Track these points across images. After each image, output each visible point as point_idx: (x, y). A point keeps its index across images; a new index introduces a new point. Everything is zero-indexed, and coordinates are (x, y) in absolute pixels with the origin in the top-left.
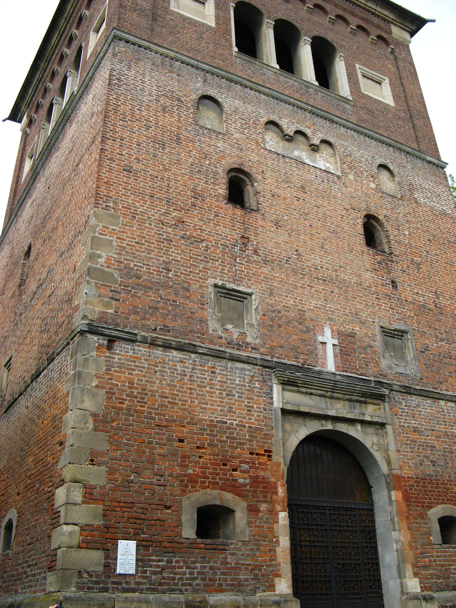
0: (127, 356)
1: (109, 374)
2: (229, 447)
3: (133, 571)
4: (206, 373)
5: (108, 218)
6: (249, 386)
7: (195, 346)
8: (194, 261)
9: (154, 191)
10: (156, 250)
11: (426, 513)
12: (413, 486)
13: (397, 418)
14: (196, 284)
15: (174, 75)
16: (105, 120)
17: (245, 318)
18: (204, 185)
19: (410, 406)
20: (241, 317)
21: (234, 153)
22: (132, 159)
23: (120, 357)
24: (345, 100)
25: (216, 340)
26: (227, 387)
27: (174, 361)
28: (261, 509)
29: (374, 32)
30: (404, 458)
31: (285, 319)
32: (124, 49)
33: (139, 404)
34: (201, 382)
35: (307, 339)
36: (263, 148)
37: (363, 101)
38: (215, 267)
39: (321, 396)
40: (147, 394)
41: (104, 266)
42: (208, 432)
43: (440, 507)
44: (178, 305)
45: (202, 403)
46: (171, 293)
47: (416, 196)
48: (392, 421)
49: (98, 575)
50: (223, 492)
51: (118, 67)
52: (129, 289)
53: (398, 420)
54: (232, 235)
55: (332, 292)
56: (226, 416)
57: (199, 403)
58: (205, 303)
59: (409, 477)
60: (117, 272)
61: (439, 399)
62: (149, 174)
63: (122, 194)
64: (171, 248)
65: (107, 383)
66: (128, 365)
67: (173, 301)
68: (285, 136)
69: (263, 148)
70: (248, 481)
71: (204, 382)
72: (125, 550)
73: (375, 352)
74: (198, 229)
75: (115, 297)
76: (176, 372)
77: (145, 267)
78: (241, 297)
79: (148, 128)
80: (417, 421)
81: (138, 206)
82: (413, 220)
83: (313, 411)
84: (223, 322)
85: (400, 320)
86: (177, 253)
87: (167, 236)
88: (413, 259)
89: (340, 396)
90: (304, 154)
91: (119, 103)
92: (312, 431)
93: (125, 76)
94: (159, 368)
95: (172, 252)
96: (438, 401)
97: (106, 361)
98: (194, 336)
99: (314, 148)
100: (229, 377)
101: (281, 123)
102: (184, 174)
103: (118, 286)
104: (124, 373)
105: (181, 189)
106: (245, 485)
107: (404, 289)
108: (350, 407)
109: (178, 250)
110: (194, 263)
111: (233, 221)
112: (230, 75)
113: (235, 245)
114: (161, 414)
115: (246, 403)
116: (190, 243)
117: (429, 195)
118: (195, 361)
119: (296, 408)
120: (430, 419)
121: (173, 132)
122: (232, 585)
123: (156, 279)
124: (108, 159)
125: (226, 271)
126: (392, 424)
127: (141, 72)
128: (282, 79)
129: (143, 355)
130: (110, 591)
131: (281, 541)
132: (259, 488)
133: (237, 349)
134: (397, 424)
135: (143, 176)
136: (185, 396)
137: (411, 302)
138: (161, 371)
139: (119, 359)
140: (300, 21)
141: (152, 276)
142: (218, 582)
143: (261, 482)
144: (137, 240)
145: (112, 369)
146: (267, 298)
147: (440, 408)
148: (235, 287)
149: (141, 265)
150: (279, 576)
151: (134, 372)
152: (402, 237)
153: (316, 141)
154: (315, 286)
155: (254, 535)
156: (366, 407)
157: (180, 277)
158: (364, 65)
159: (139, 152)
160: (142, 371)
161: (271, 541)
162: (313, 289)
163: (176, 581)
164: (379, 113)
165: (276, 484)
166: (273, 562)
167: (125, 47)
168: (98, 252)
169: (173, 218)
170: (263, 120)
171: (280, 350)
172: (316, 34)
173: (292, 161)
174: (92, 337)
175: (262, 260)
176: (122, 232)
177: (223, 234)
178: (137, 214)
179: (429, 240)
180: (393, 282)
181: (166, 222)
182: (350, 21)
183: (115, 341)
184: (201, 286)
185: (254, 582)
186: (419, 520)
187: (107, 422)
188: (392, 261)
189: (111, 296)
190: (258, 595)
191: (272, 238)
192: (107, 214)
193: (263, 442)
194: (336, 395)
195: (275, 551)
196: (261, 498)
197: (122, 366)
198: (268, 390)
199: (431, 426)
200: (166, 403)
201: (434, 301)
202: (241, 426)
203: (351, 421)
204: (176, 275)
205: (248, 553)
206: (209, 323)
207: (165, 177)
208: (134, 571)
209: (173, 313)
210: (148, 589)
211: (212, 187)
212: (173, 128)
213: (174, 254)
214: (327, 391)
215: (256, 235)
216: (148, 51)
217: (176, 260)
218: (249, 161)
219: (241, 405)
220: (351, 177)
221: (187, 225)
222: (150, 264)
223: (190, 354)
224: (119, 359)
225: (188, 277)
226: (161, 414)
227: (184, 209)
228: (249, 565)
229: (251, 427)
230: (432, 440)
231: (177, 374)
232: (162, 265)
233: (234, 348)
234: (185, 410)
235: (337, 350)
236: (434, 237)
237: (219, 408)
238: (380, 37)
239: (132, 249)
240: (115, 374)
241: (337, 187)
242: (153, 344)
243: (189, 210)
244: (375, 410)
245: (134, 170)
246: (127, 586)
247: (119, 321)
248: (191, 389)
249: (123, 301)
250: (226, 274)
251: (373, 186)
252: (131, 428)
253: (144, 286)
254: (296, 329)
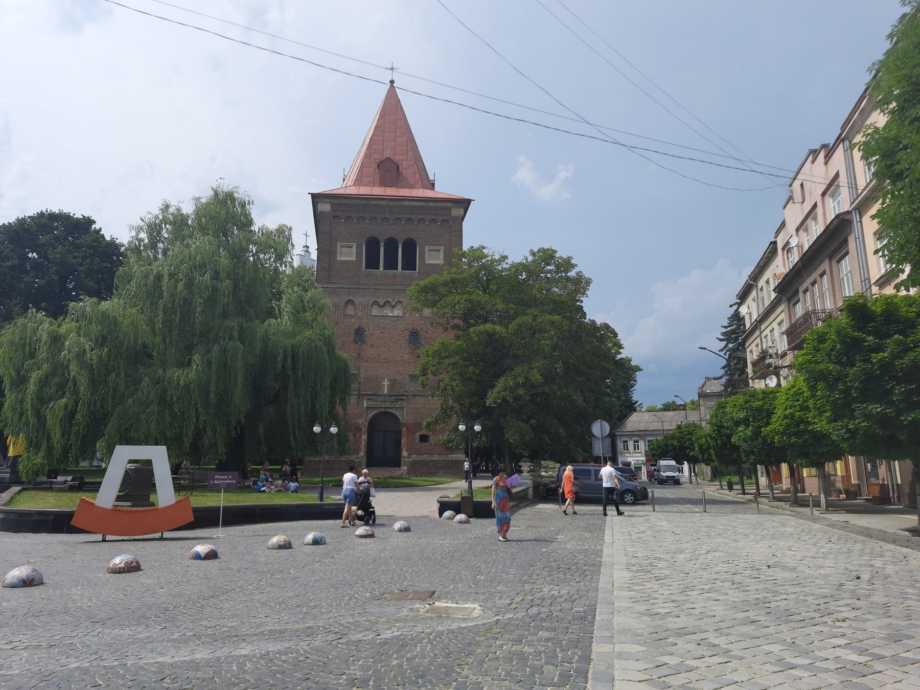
99: (393, 307)
153: (393, 304)
203: (392, 408)
251: (418, 315)
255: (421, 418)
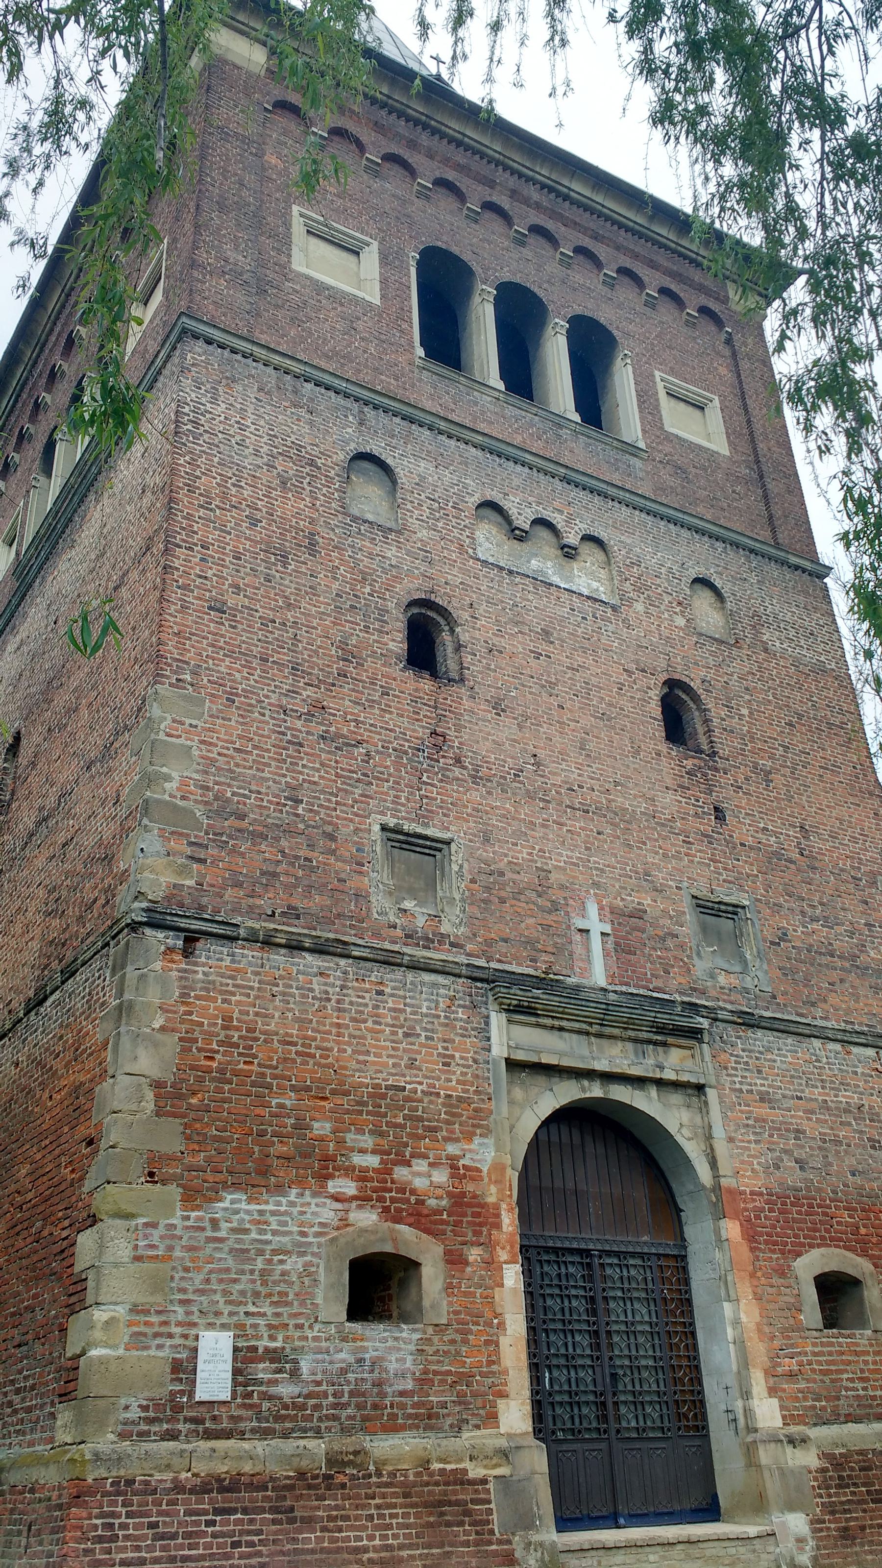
0: (221, 968)
1: (187, 1004)
2: (409, 1135)
3: (226, 1396)
4: (367, 995)
5: (182, 703)
6: (446, 1017)
7: (345, 943)
8: (343, 783)
9: (267, 649)
10: (273, 763)
11: (789, 1266)
12: (762, 1210)
13: (728, 1075)
14: (348, 826)
15: (302, 412)
16: (171, 508)
17: (438, 888)
18: (361, 634)
19: (750, 1051)
20: (431, 886)
21: (417, 568)
22: (226, 587)
23: (206, 969)
24: (631, 449)
25: (385, 932)
26: (405, 1020)
27: (308, 974)
28: (471, 1259)
29: (693, 301)
30: (742, 1154)
31: (511, 888)
32: (203, 358)
33: (242, 1059)
34: (357, 1012)
35: (553, 924)
36: (471, 557)
37: (668, 449)
38: (382, 793)
39: (579, 1032)
40: (256, 1039)
41: (175, 797)
42: (371, 1108)
43: (816, 1253)
44: (314, 867)
45: (360, 1053)
46: (302, 844)
47: (765, 638)
48: (718, 1081)
49: (159, 1404)
50: (398, 1226)
51: (193, 395)
52: (224, 838)
53: (729, 1079)
54: (414, 731)
55: (599, 833)
56: (404, 1076)
57: (354, 1052)
58: (365, 862)
59: (752, 1193)
60: (201, 807)
61: (810, 1036)
62: (258, 615)
63: (207, 656)
64: (302, 759)
65: (182, 1022)
66: (221, 985)
67: (306, 859)
68: (513, 531)
69: (471, 557)
70: (444, 1203)
71: (362, 1012)
72: (211, 1352)
73: (682, 946)
74: (351, 720)
75: (196, 855)
76: (311, 995)
77: (254, 796)
78: (430, 848)
79: (254, 522)
80: (766, 1079)
81: (239, 679)
82: (759, 685)
83: (566, 1062)
84: (396, 893)
85: (730, 882)
86: (313, 768)
87: (293, 735)
88: (758, 764)
89: (616, 1032)
90: (549, 564)
91: (198, 473)
92: (564, 1100)
93: (208, 416)
94: (281, 988)
95: (304, 766)
96: (807, 1040)
97: (181, 978)
98: (344, 926)
99: (569, 553)
100: (408, 1000)
101: (505, 504)
102: (323, 613)
103: (202, 834)
104: (215, 1000)
105: (319, 643)
106: (439, 1212)
107: (740, 822)
108: (636, 1053)
109: (314, 762)
110: (345, 787)
111: (416, 702)
112: (410, 410)
113: (419, 750)
114: (283, 1077)
115: (440, 1050)
116: (336, 748)
117: (792, 633)
118: (345, 973)
119: (534, 1059)
120: (792, 1077)
121: (303, 531)
122: (416, 1416)
123: (274, 818)
124: (179, 587)
125: (403, 800)
126: (718, 1087)
127: (239, 406)
128: (510, 411)
129: (250, 964)
130: (182, 1438)
131: (508, 1322)
132: (466, 1215)
133: (424, 947)
134: (728, 1085)
135: (246, 619)
136: (328, 1040)
137: (751, 848)
138: (284, 994)
139: (204, 973)
140: (545, 286)
141: (266, 812)
142: (389, 1410)
143: (470, 1205)
144: (237, 746)
145: (192, 994)
146: (478, 849)
147: (812, 1054)
148: (420, 830)
149: (246, 792)
150: (504, 1395)
151: (233, 998)
152: (737, 720)
153: (572, 539)
154: (569, 822)
155: (456, 1313)
156: (665, 1052)
157: (318, 813)
158: (672, 372)
159: (238, 571)
160: (248, 996)
161: (490, 1324)
162: (565, 829)
163: (309, 1412)
164: (698, 471)
165: (497, 1207)
166: (494, 1368)
167: (205, 353)
168: (164, 770)
169: (304, 700)
170: (472, 500)
171: (502, 947)
172: (579, 310)
173: (527, 581)
174: (154, 933)
175: (469, 775)
176: (209, 730)
177: (397, 729)
178: (237, 695)
179: (790, 724)
180: (716, 809)
181: (292, 710)
182: (646, 279)
183: (198, 939)
184: (357, 829)
185: (457, 1409)
186: (776, 1280)
187: (180, 1097)
188: (716, 770)
189: (189, 853)
190: (466, 1435)
191: (489, 734)
192: (180, 696)
193: (473, 1126)
194: (608, 1030)
195: (497, 1345)
196: (470, 1237)
197: (211, 986)
198: (480, 1023)
199: (795, 1090)
200: (293, 1056)
201: (799, 843)
202: (431, 1094)
203: (639, 1082)
204: (311, 811)
205: (446, 1348)
206: (373, 899)
207: (288, 620)
208: (229, 1394)
209: (306, 883)
210: (253, 1431)
211: (375, 637)
212: (302, 523)
213: (306, 771)
214: (591, 1024)
215: (459, 728)
216: (249, 361)
217: (310, 782)
218: (446, 583)
219: (432, 1055)
220: (639, 607)
221: (330, 714)
222: (263, 790)
223: (337, 959)
224: (204, 973)
225: (334, 813)
226: (283, 1077)
227: (324, 682)
228: (449, 1373)
229: (450, 1096)
230: (797, 1117)
231: (313, 998)
232: (284, 791)
233: (418, 945)
234: (329, 1066)
235: (610, 945)
236: (800, 716)
237: (391, 1061)
238: (704, 310)
239: (229, 763)
240: (198, 1002)
241: (611, 628)
242: (268, 943)
243: (334, 685)
244: (682, 1060)
245: (230, 608)
246: (214, 1427)
247: (204, 901)
248: (338, 1026)
249: (211, 863)
250: (403, 805)
251: (681, 621)
252: (226, 1106)
253: (252, 833)
254: (532, 907)
255: (801, 1164)
